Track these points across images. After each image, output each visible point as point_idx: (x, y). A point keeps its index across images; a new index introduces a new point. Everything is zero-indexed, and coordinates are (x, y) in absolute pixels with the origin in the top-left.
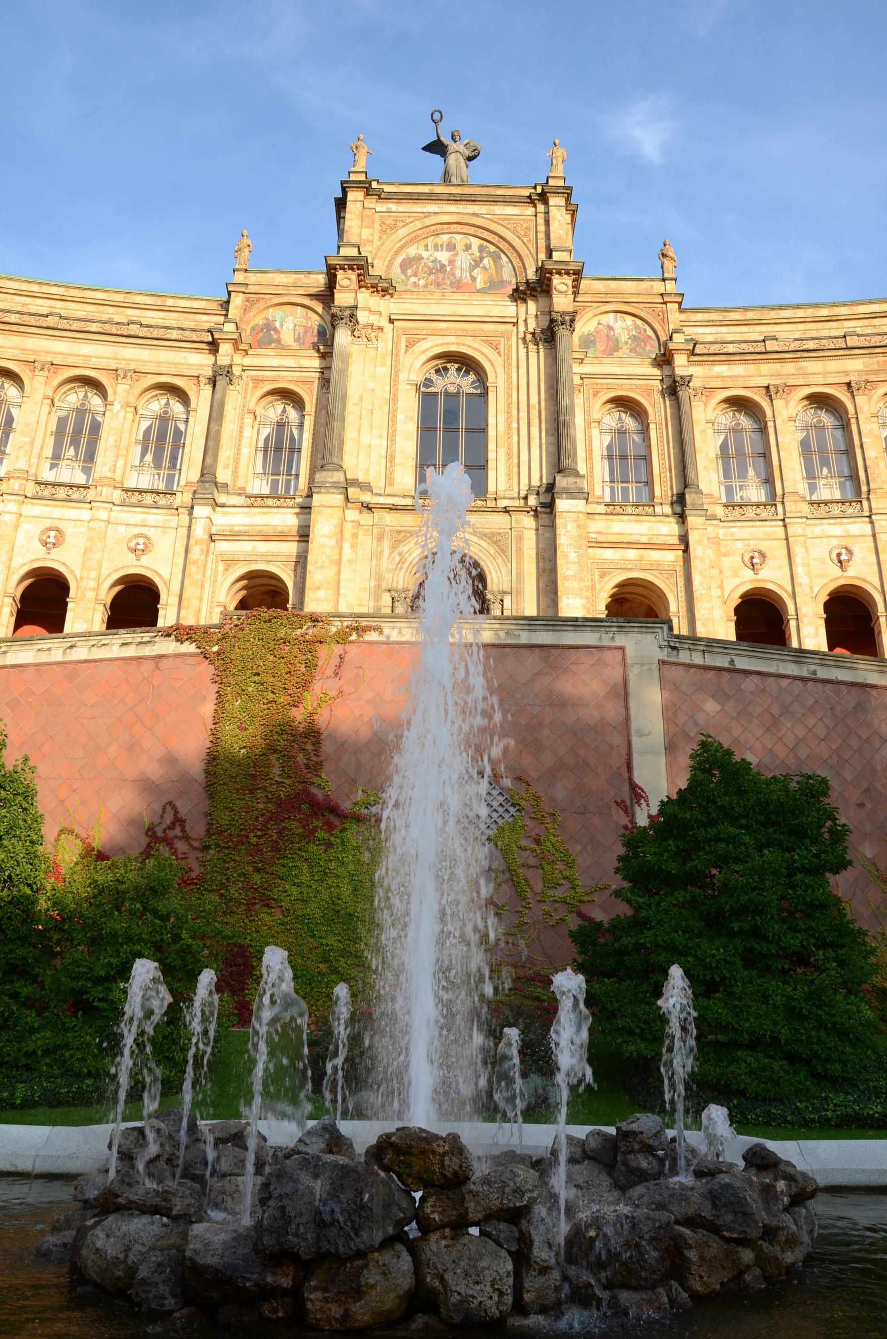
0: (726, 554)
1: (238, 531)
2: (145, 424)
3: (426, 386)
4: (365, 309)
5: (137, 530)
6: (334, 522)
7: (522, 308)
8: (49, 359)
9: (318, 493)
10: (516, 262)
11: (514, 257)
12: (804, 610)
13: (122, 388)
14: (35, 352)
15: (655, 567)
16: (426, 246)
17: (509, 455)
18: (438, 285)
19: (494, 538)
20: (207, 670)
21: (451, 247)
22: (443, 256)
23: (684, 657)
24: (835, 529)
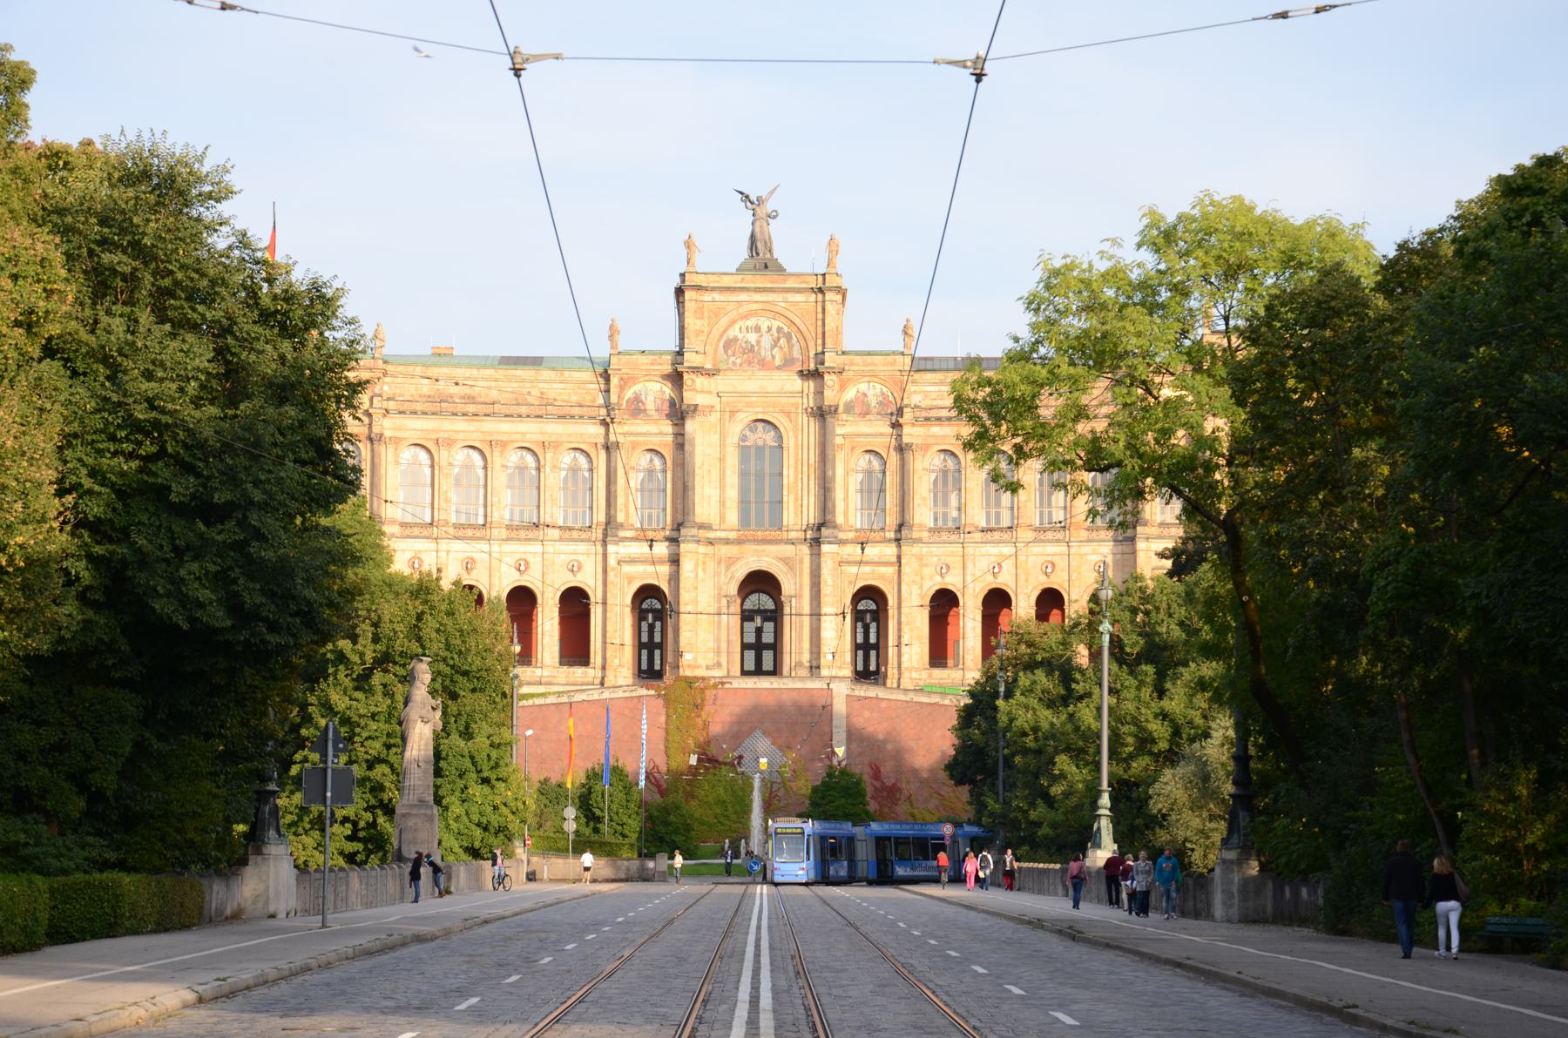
0: (926, 565)
2: (563, 474)
3: (744, 441)
4: (702, 392)
5: (572, 557)
6: (694, 562)
7: (806, 384)
8: (500, 438)
10: (802, 342)
11: (801, 338)
13: (549, 455)
14: (491, 433)
15: (882, 577)
17: (796, 499)
18: (750, 363)
19: (786, 561)
20: (660, 701)
21: (758, 329)
22: (753, 337)
23: (857, 693)
24: (993, 550)
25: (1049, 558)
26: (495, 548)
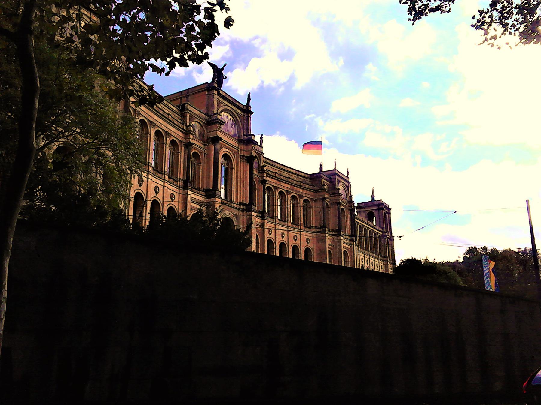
1: (193, 200)
9: (217, 197)
12: (277, 247)
16: (223, 114)
18: (225, 130)
19: (235, 215)
21: (227, 117)
22: (226, 120)
24: (282, 228)
25: (295, 234)
26: (150, 177)
